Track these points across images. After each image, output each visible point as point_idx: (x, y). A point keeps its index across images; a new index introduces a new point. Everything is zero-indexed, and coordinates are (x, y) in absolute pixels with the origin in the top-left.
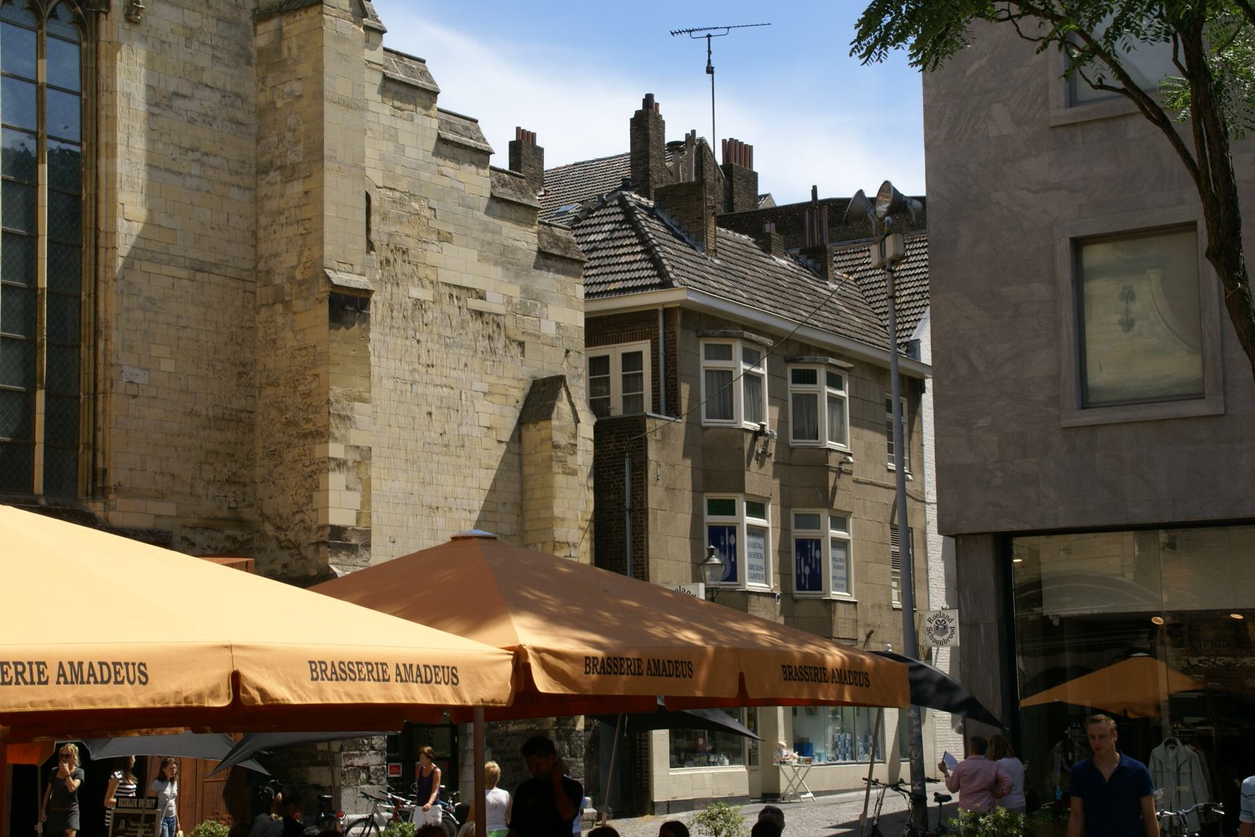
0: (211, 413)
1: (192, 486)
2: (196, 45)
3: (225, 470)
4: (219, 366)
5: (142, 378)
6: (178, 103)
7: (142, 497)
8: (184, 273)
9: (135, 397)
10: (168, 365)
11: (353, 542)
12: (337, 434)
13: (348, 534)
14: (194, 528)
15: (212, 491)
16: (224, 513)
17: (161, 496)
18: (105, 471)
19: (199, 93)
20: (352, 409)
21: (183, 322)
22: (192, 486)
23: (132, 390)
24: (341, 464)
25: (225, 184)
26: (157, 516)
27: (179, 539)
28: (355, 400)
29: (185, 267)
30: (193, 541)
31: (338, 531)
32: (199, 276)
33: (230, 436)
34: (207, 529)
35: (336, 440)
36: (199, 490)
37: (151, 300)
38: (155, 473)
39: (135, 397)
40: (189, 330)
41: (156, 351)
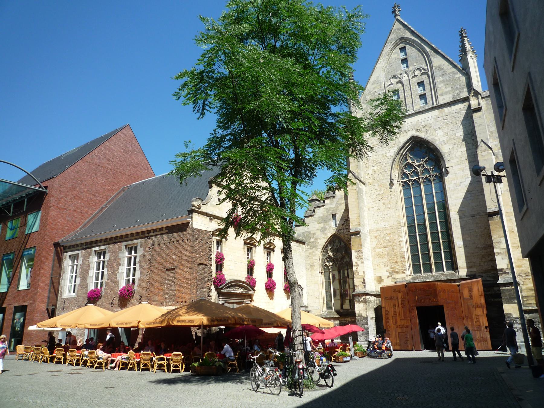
0: (482, 246)
1: (480, 263)
2: (464, 170)
3: (489, 258)
4: (483, 236)
6: (462, 184)
8: (469, 218)
11: (507, 272)
12: (496, 247)
13: (504, 270)
14: (482, 273)
15: (486, 264)
16: (490, 268)
19: (467, 180)
20: (501, 240)
24: (499, 254)
25: (477, 196)
28: (501, 237)
31: (501, 270)
32: (473, 217)
33: (489, 250)
34: (486, 272)
35: (496, 248)
36: (482, 264)
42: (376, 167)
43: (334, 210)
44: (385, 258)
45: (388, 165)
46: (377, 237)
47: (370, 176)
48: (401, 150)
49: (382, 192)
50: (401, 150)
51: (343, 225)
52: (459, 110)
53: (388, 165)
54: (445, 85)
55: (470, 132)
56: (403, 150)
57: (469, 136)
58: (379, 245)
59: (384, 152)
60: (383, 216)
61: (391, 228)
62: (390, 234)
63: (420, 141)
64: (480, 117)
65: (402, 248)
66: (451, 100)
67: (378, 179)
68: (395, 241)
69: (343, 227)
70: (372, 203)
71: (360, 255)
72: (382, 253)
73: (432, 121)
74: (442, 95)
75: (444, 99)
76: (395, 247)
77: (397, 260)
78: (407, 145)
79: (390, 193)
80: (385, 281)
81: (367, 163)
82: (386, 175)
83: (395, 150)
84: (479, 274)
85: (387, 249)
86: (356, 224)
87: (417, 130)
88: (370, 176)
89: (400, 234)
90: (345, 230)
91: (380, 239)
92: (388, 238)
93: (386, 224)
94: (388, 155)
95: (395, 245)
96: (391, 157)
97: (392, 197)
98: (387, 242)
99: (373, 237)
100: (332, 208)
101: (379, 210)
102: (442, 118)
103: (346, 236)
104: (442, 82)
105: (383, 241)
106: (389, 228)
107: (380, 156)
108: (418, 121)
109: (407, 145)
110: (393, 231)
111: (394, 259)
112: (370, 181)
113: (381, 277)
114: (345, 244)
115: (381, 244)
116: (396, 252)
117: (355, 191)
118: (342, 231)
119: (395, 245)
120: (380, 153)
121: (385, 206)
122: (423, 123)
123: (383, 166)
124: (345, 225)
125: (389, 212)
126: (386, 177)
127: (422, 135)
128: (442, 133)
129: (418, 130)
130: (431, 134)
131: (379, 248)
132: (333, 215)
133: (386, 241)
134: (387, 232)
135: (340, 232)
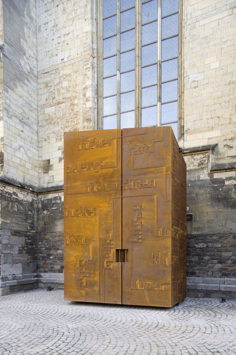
1: (230, 119)
5: (200, 77)
7: (200, 132)
8: (226, 13)
9: (195, 88)
10: (216, 65)
17: (212, 129)
18: (184, 126)
21: (224, 40)
22: (230, 119)
23: (195, 84)
26: (209, 139)
27: (223, 146)
29: (228, 10)
30: (231, 146)
37: (206, 38)
38: (208, 119)
39: (195, 88)
40: (229, 42)
41: (207, 61)
44: (58, 124)
46: (49, 85)
58: (51, 101)
61: (73, 62)
62: (69, 75)
65: (87, 100)
68: (77, 89)
72: (54, 116)
76: (76, 101)
80: (55, 167)
84: (225, 143)
89: (87, 73)
91: (52, 89)
95: (75, 97)
99: (42, 86)
101: (55, 29)
106: (69, 63)
110: (75, 68)
111: (73, 124)
113: (49, 161)
115: (54, 98)
131: (51, 106)
133: (62, 91)
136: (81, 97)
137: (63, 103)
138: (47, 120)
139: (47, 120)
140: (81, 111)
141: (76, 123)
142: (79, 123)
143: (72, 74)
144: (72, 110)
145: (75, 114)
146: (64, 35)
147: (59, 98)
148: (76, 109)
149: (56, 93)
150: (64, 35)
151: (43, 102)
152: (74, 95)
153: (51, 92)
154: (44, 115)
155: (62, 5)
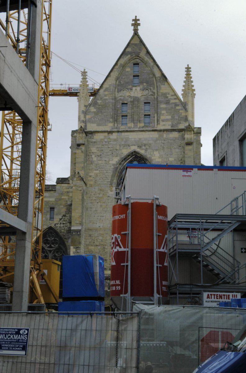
42: (98, 172)
43: (53, 204)
45: (109, 171)
46: (92, 236)
47: (92, 178)
48: (122, 161)
49: (101, 195)
50: (122, 161)
51: (60, 219)
52: (174, 139)
53: (109, 171)
54: (167, 112)
55: (180, 159)
56: (124, 161)
57: (179, 162)
59: (107, 160)
60: (100, 218)
62: (103, 234)
63: (140, 157)
64: (190, 150)
66: (170, 128)
67: (99, 183)
69: (61, 221)
70: (91, 204)
71: (78, 251)
72: (94, 251)
73: (151, 142)
74: (163, 121)
75: (164, 125)
76: (106, 247)
77: (107, 258)
78: (129, 158)
79: (108, 198)
81: (91, 165)
82: (106, 180)
83: (117, 160)
85: (99, 247)
86: (78, 222)
87: (138, 146)
88: (92, 178)
90: (62, 225)
92: (101, 238)
93: (101, 225)
94: (111, 162)
95: (106, 245)
96: (113, 165)
97: (109, 201)
98: (100, 241)
100: (51, 201)
102: (160, 142)
103: (63, 231)
104: (165, 109)
105: (97, 239)
107: (104, 162)
108: (140, 139)
109: (129, 158)
112: (92, 183)
114: (61, 238)
115: (94, 243)
116: (107, 251)
117: (80, 192)
118: (59, 225)
119: (106, 245)
120: (104, 159)
121: (102, 208)
122: (144, 142)
123: (105, 172)
124: (62, 220)
125: (104, 215)
126: (106, 182)
127: (142, 152)
128: (158, 155)
129: (140, 147)
130: (149, 153)
131: (92, 246)
132: (51, 208)
134: (101, 232)
135: (57, 225)
136: (109, 245)
137: (99, 246)
138: (90, 252)
139: (90, 252)
140: (109, 252)
141: (106, 256)
142: (107, 257)
143: (105, 234)
144: (104, 250)
145: (105, 253)
146: (101, 216)
147: (98, 244)
148: (106, 250)
149: (96, 240)
150: (101, 216)
151: (88, 243)
152: (106, 244)
153: (93, 239)
154: (88, 249)
155: (100, 203)
